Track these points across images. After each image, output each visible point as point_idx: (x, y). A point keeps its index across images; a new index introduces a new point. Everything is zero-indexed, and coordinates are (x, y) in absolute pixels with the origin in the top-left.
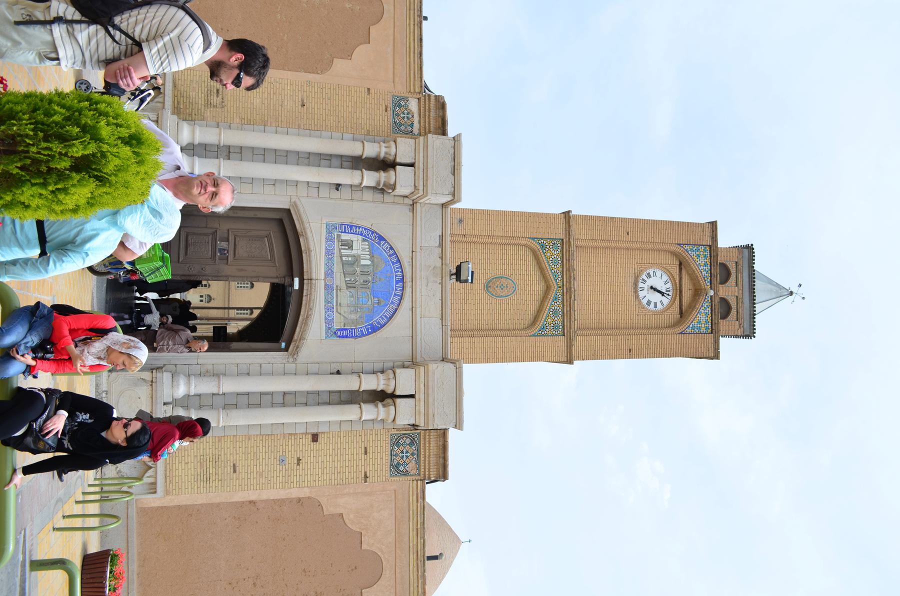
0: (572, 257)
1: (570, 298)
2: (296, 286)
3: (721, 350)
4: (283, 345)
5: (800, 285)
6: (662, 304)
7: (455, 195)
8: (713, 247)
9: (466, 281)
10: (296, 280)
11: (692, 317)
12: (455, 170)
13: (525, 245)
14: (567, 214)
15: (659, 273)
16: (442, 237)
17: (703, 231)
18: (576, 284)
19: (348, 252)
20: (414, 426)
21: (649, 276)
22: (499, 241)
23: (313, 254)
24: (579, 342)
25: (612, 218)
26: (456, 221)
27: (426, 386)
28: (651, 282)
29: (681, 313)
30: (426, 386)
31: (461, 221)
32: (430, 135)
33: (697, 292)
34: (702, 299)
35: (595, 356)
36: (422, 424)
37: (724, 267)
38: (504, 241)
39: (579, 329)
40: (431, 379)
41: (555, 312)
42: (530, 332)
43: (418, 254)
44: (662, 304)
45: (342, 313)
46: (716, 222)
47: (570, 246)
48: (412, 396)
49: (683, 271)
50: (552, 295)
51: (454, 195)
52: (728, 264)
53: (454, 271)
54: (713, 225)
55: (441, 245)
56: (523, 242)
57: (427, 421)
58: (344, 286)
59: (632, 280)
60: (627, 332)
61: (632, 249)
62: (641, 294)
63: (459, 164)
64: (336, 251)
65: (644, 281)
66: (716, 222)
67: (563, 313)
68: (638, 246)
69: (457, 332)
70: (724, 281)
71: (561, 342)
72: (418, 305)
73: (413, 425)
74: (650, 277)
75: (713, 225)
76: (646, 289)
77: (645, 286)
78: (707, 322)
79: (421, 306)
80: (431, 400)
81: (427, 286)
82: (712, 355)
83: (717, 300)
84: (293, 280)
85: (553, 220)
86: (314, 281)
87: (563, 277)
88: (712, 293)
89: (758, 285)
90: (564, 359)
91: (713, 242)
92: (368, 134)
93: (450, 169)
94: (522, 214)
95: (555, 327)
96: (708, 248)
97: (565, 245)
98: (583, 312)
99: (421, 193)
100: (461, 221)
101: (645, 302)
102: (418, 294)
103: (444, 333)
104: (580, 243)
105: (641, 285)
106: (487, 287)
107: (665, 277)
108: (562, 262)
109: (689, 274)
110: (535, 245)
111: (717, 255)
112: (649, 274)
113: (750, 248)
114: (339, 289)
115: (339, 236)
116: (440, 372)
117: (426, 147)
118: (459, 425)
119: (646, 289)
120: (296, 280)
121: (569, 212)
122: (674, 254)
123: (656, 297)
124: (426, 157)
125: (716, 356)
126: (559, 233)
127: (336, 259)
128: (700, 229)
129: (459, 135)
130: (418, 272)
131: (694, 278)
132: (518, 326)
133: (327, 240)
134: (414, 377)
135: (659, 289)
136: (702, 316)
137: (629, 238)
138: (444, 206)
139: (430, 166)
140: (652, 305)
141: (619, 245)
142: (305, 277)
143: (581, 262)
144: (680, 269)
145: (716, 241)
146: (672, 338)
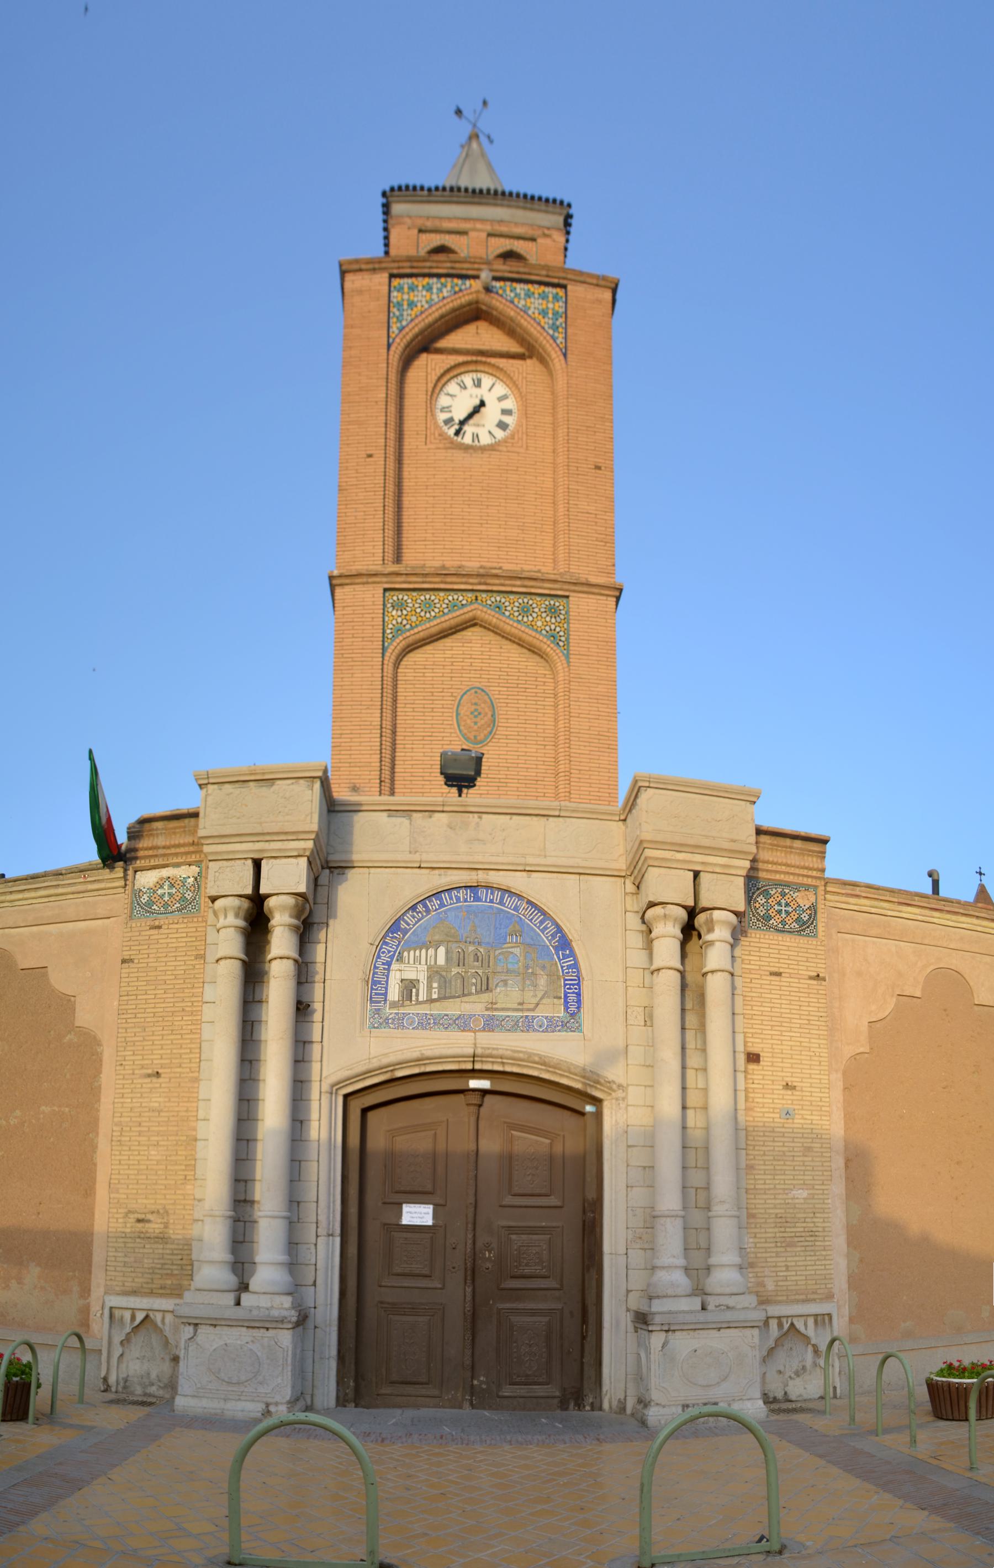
2: (484, 1084)
4: (589, 1108)
10: (474, 1084)
13: (397, 664)
18: (472, 565)
19: (423, 988)
23: (429, 1053)
45: (535, 1001)
50: (490, 616)
56: (389, 668)
58: (486, 997)
64: (424, 1010)
78: (544, 296)
84: (474, 1090)
86: (479, 1051)
92: (203, 957)
114: (491, 1006)
115: (394, 1005)
120: (474, 1084)
121: (331, 578)
122: (407, 361)
127: (437, 1009)
133: (401, 1026)
142: (469, 1066)
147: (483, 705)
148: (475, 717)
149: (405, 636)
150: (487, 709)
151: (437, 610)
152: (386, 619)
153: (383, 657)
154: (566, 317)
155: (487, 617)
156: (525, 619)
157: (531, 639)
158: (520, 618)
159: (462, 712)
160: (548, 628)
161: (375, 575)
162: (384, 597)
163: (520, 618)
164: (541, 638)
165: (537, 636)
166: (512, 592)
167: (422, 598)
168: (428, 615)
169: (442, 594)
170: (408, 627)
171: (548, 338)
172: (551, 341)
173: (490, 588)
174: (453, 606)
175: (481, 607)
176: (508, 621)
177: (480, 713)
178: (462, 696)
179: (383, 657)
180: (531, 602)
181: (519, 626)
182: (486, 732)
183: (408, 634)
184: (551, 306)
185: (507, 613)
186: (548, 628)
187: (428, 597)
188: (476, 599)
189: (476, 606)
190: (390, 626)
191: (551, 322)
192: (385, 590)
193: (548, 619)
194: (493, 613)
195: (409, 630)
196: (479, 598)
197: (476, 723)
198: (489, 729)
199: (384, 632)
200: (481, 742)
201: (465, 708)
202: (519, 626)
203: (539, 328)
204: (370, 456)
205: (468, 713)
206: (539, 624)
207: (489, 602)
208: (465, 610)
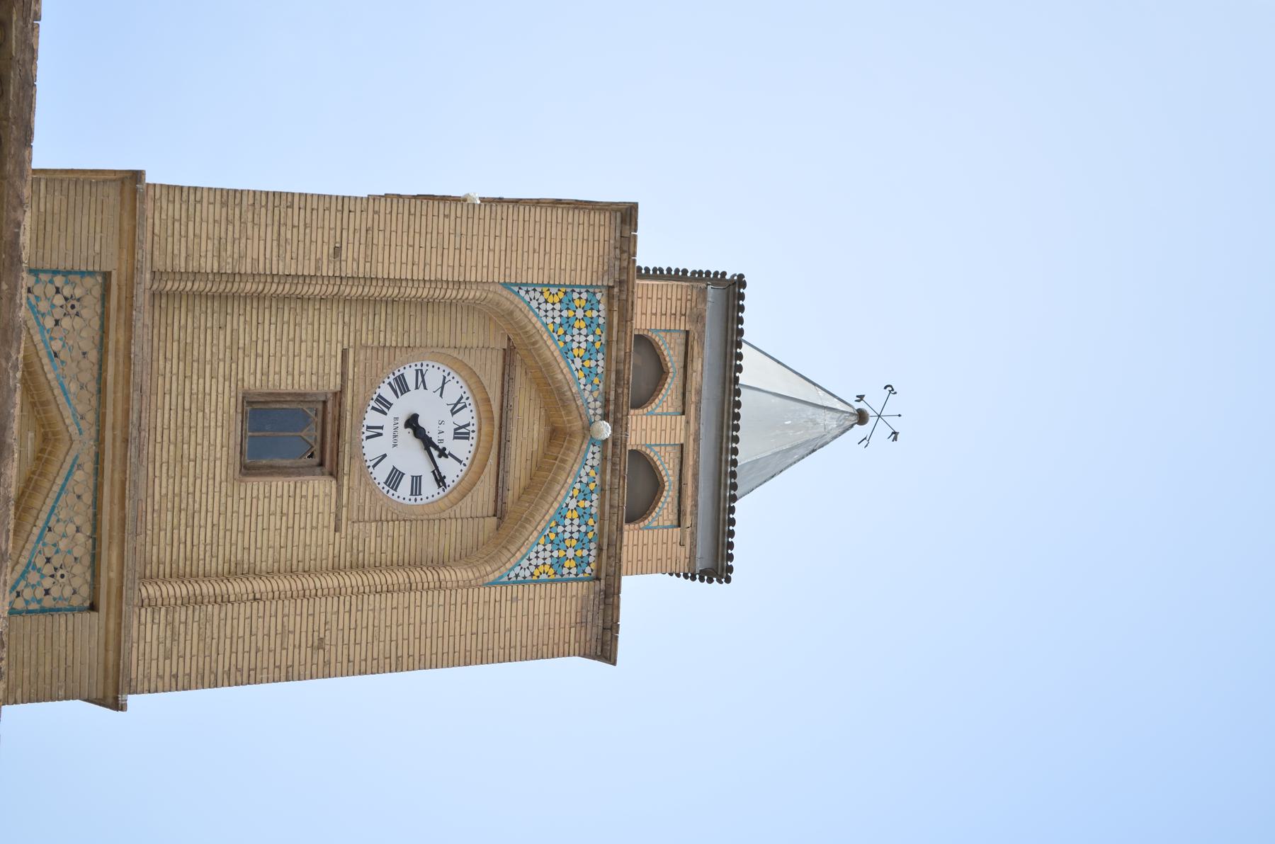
24: (147, 633)
29: (499, 513)
44: (440, 480)
49: (519, 373)
76: (387, 432)
77: (385, 421)
101: (381, 474)
107: (455, 389)
112: (401, 381)
140: (405, 486)
184: (570, 553)
192: (107, 276)
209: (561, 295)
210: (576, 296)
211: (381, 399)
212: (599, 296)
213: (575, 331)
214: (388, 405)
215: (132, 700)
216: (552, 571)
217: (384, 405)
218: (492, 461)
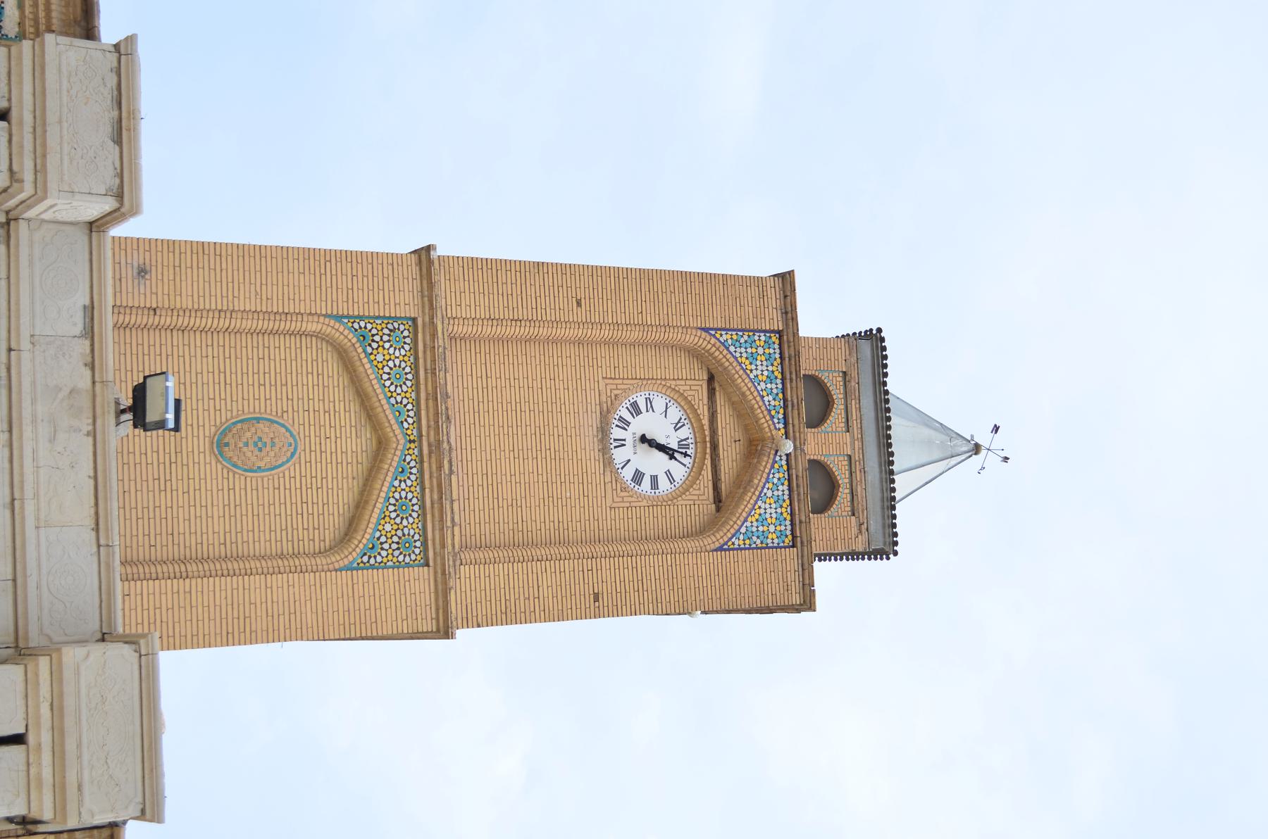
0: (439, 364)
1: (440, 467)
3: (818, 587)
5: (996, 429)
6: (671, 478)
7: (124, 198)
8: (786, 335)
9: (161, 425)
11: (743, 509)
12: (122, 130)
13: (317, 335)
14: (424, 254)
15: (659, 402)
16: (90, 311)
17: (762, 296)
20: (26, 822)
21: (635, 409)
22: (247, 324)
24: (468, 582)
25: (538, 265)
26: (130, 273)
27: (57, 708)
28: (641, 425)
29: (718, 500)
30: (57, 708)
31: (142, 272)
32: (49, 38)
33: (754, 447)
34: (765, 463)
35: (508, 616)
36: (47, 815)
37: (816, 384)
38: (262, 325)
39: (465, 547)
40: (69, 688)
41: (401, 506)
42: (338, 560)
43: (26, 356)
44: (671, 478)
46: (791, 273)
47: (434, 335)
48: (17, 739)
50: (392, 462)
51: (120, 196)
52: (826, 378)
53: (127, 401)
54: (786, 280)
55: (90, 332)
56: (313, 327)
57: (61, 807)
59: (595, 420)
60: (586, 550)
61: (592, 343)
62: (619, 456)
63: (134, 115)
65: (624, 424)
66: (791, 273)
67: (423, 507)
68: (606, 333)
69: (139, 567)
70: (818, 419)
71: (420, 582)
72: (29, 492)
73: (24, 821)
74: (638, 412)
75: (786, 280)
76: (629, 442)
77: (628, 435)
79: (36, 496)
80: (70, 745)
81: (52, 440)
82: (796, 599)
83: (801, 466)
85: (387, 271)
87: (418, 414)
88: (788, 447)
89: (899, 428)
90: (429, 626)
91: (787, 325)
93: (106, 129)
94: (309, 254)
95: (403, 544)
96: (775, 338)
97: (422, 334)
98: (474, 506)
99: (28, 190)
100: (142, 272)
101: (628, 474)
102: (28, 462)
103: (103, 568)
104: (460, 329)
105: (616, 433)
106: (220, 445)
107: (675, 413)
108: (416, 376)
109: (733, 404)
110: (346, 337)
111: (797, 354)
113: (875, 338)
116: (96, 670)
117: (39, 68)
118: (151, 810)
119: (629, 442)
121: (428, 249)
122: (695, 354)
123: (655, 463)
124: (40, 94)
125: (807, 603)
126: (406, 303)
128: (754, 291)
129: (131, 40)
130: (26, 404)
131: (743, 412)
132: (308, 547)
134: (20, 687)
135: (662, 441)
136: (767, 507)
137: (580, 315)
138: (95, 227)
139: (51, 117)
140: (646, 482)
141: (560, 332)
143: (463, 377)
144: (712, 392)
145: (794, 319)
146: (697, 562)
147: (272, 454)
148: (256, 445)
149: (357, 345)
150: (267, 459)
151: (392, 388)
152: (379, 322)
153: (326, 316)
154: (761, 548)
155: (390, 456)
156: (391, 508)
157: (367, 517)
158: (392, 501)
159: (261, 425)
160: (383, 539)
161: (431, 307)
162: (405, 318)
163: (392, 501)
164: (369, 530)
165: (371, 525)
166: (423, 489)
167: (408, 369)
168: (386, 377)
169: (413, 395)
170: (369, 350)
171: (736, 527)
172: (732, 531)
173: (426, 459)
174: (398, 409)
175: (400, 447)
176: (386, 484)
177: (260, 450)
178: (283, 426)
179: (326, 316)
180: (415, 515)
181: (381, 500)
182: (235, 459)
183: (360, 350)
184: (772, 528)
185: (396, 483)
186: (383, 539)
187: (410, 377)
188: (410, 441)
189: (402, 442)
190: (369, 326)
191: (754, 529)
192: (414, 320)
193: (395, 539)
194: (394, 464)
195: (364, 351)
196: (412, 445)
197: (247, 445)
198: (239, 463)
199: (361, 318)
200: (221, 453)
201: (267, 430)
202: (381, 500)
203: (744, 514)
204: (579, 304)
205: (259, 434)
206: (388, 527)
207: (408, 459)
208: (395, 427)
209: (746, 337)
210: (756, 338)
211: (621, 419)
212: (774, 339)
213: (759, 363)
214: (628, 424)
215: (459, 633)
216: (758, 542)
217: (624, 424)
218: (708, 462)
